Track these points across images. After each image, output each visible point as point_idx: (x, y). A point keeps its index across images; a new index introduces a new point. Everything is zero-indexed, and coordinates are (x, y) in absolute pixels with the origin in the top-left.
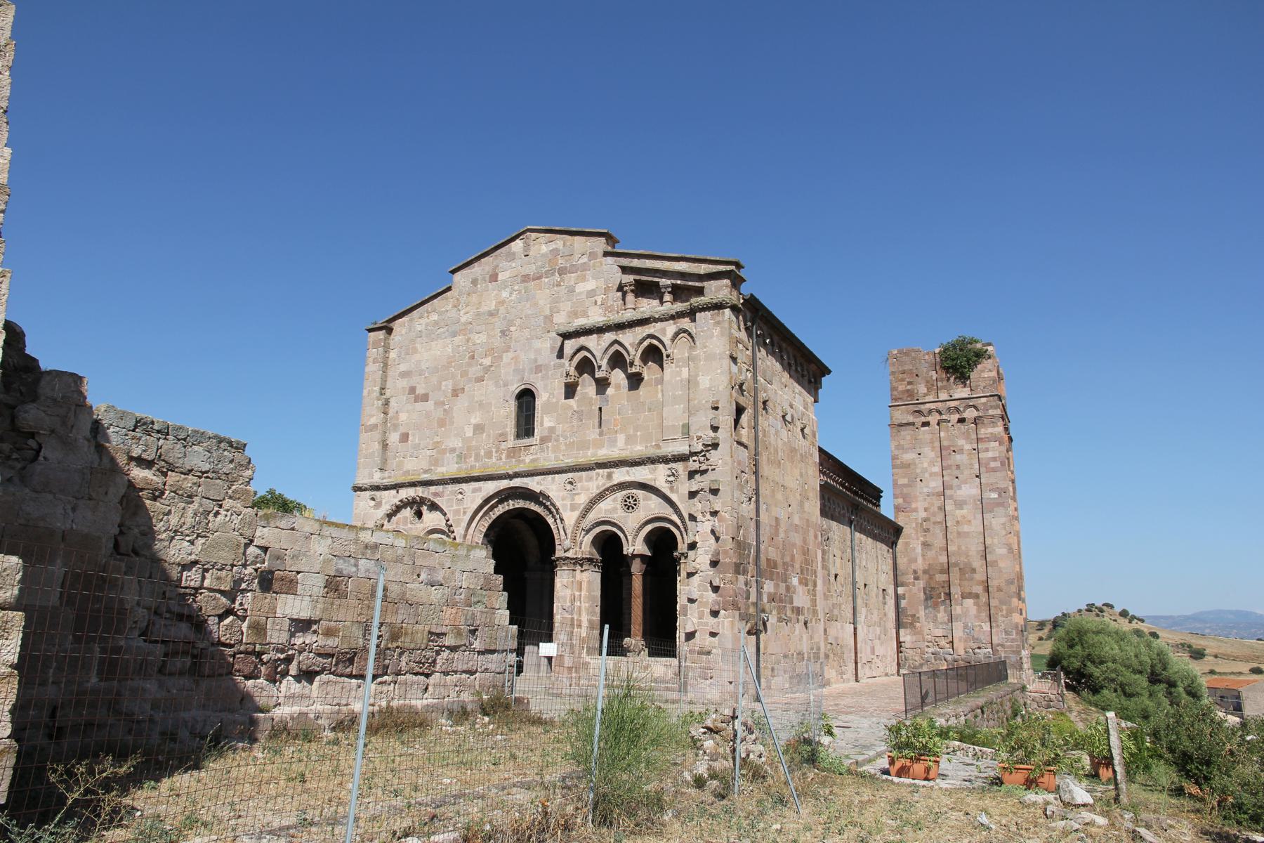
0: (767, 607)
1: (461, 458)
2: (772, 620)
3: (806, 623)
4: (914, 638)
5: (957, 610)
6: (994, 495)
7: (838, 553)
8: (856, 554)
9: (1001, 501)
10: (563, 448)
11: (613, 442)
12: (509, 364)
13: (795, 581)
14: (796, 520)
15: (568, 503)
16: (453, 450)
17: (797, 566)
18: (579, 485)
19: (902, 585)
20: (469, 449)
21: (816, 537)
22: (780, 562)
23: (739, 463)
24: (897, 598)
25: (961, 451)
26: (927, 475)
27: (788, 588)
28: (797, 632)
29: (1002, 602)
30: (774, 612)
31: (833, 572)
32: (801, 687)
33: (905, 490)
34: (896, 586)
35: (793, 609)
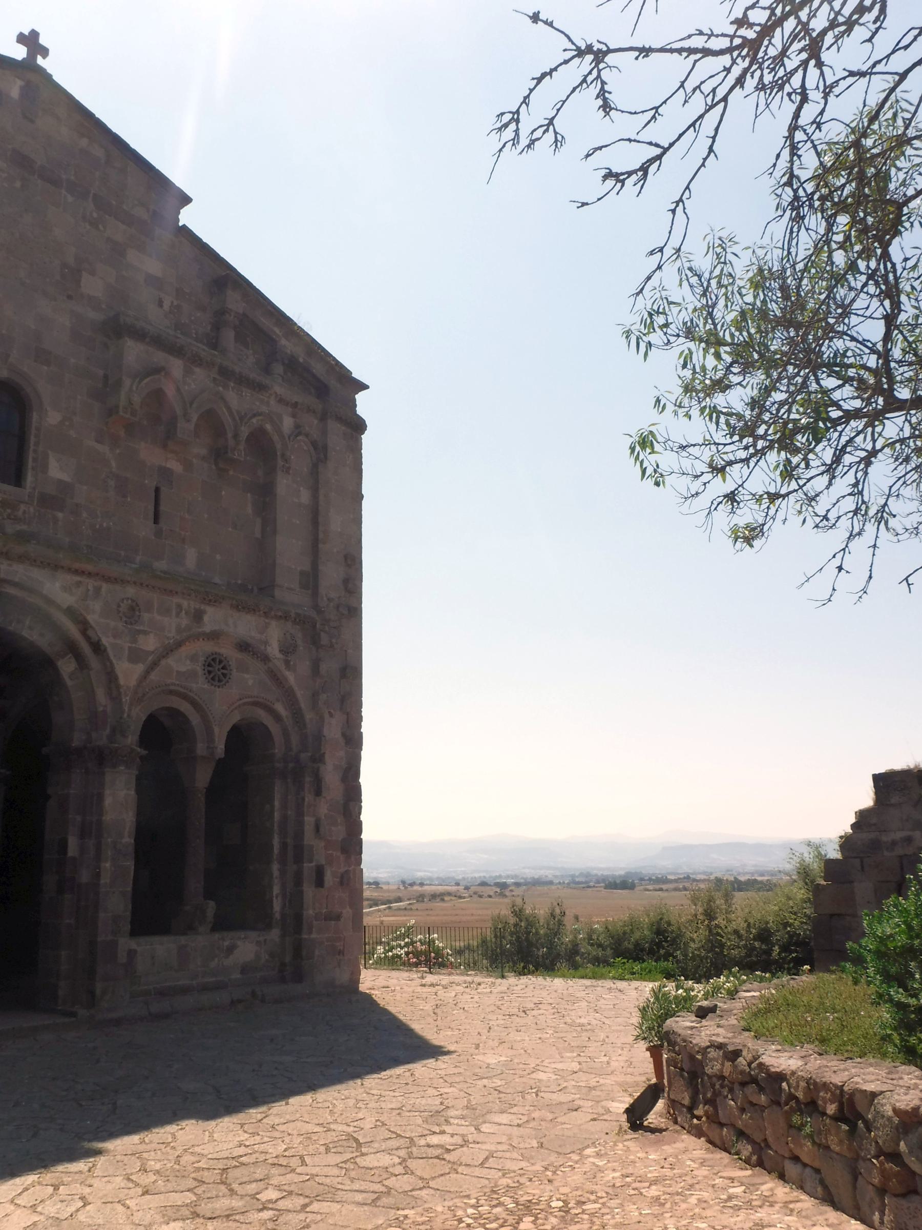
18: (146, 616)
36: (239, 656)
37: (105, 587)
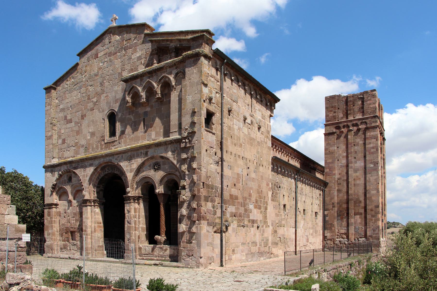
0: (230, 219)
1: (86, 149)
2: (233, 225)
3: (258, 227)
5: (352, 220)
7: (286, 194)
8: (298, 195)
10: (128, 141)
11: (150, 136)
12: (104, 100)
13: (251, 207)
14: (253, 175)
15: (129, 168)
16: (83, 146)
17: (253, 199)
19: (327, 210)
20: (89, 144)
21: (268, 185)
22: (240, 196)
23: (209, 142)
24: (324, 216)
27: (246, 210)
28: (252, 232)
30: (235, 222)
31: (282, 203)
32: (254, 259)
34: (324, 209)
35: (249, 221)
36: (163, 160)
37: (124, 155)
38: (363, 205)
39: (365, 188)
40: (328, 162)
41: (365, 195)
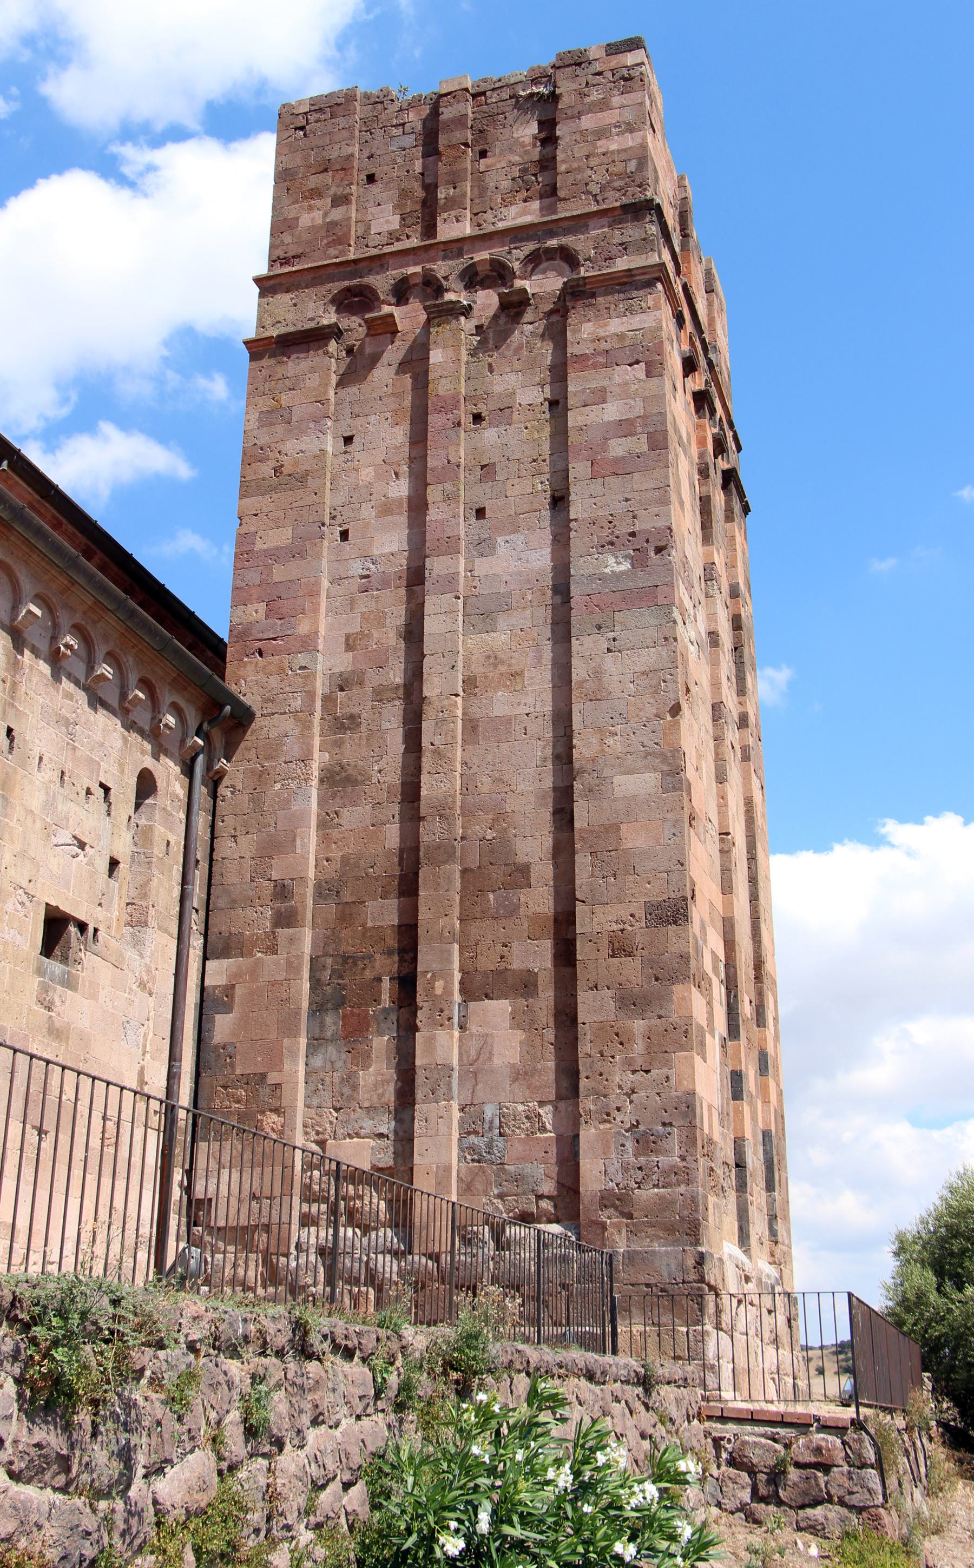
4: (252, 1181)
5: (441, 1046)
6: (616, 564)
9: (643, 580)
19: (225, 953)
25: (505, 411)
26: (367, 512)
29: (631, 1002)
33: (279, 573)
38: (540, 899)
39: (564, 757)
40: (259, 546)
41: (563, 814)
